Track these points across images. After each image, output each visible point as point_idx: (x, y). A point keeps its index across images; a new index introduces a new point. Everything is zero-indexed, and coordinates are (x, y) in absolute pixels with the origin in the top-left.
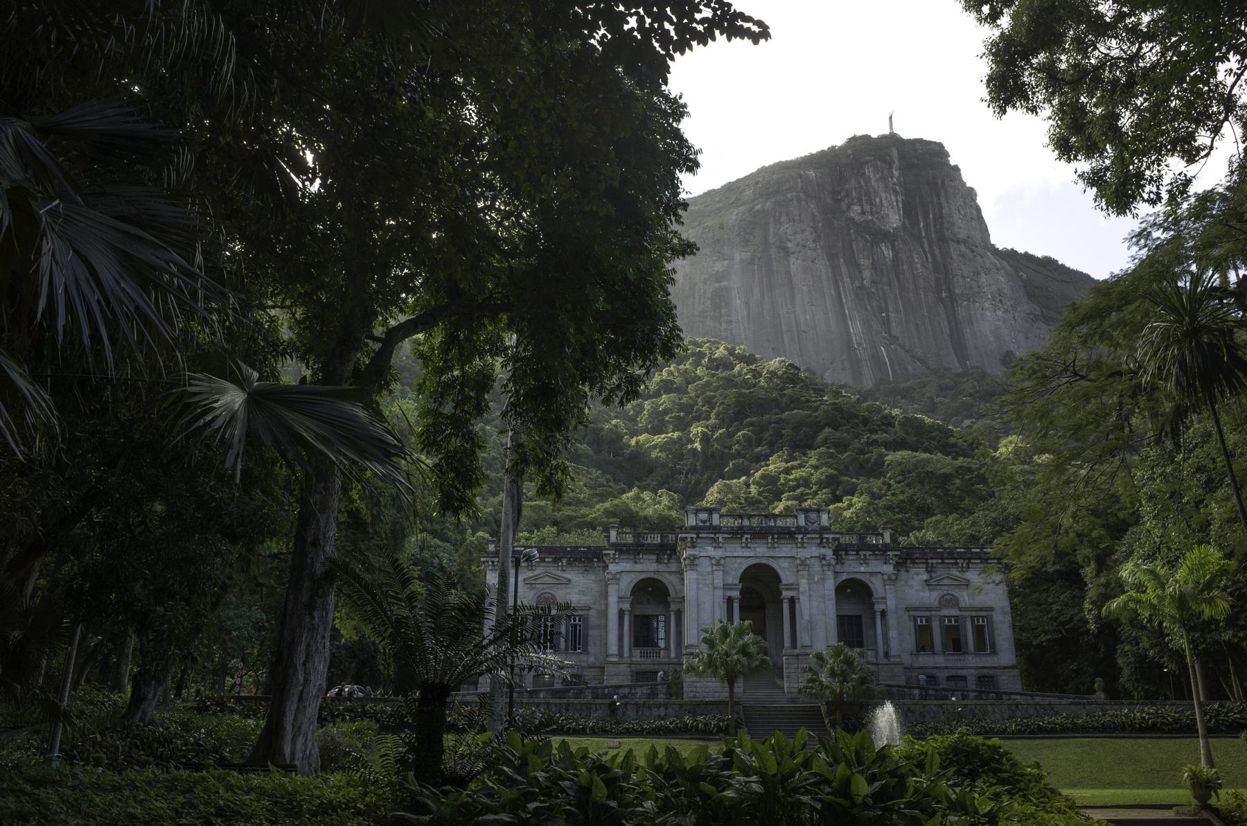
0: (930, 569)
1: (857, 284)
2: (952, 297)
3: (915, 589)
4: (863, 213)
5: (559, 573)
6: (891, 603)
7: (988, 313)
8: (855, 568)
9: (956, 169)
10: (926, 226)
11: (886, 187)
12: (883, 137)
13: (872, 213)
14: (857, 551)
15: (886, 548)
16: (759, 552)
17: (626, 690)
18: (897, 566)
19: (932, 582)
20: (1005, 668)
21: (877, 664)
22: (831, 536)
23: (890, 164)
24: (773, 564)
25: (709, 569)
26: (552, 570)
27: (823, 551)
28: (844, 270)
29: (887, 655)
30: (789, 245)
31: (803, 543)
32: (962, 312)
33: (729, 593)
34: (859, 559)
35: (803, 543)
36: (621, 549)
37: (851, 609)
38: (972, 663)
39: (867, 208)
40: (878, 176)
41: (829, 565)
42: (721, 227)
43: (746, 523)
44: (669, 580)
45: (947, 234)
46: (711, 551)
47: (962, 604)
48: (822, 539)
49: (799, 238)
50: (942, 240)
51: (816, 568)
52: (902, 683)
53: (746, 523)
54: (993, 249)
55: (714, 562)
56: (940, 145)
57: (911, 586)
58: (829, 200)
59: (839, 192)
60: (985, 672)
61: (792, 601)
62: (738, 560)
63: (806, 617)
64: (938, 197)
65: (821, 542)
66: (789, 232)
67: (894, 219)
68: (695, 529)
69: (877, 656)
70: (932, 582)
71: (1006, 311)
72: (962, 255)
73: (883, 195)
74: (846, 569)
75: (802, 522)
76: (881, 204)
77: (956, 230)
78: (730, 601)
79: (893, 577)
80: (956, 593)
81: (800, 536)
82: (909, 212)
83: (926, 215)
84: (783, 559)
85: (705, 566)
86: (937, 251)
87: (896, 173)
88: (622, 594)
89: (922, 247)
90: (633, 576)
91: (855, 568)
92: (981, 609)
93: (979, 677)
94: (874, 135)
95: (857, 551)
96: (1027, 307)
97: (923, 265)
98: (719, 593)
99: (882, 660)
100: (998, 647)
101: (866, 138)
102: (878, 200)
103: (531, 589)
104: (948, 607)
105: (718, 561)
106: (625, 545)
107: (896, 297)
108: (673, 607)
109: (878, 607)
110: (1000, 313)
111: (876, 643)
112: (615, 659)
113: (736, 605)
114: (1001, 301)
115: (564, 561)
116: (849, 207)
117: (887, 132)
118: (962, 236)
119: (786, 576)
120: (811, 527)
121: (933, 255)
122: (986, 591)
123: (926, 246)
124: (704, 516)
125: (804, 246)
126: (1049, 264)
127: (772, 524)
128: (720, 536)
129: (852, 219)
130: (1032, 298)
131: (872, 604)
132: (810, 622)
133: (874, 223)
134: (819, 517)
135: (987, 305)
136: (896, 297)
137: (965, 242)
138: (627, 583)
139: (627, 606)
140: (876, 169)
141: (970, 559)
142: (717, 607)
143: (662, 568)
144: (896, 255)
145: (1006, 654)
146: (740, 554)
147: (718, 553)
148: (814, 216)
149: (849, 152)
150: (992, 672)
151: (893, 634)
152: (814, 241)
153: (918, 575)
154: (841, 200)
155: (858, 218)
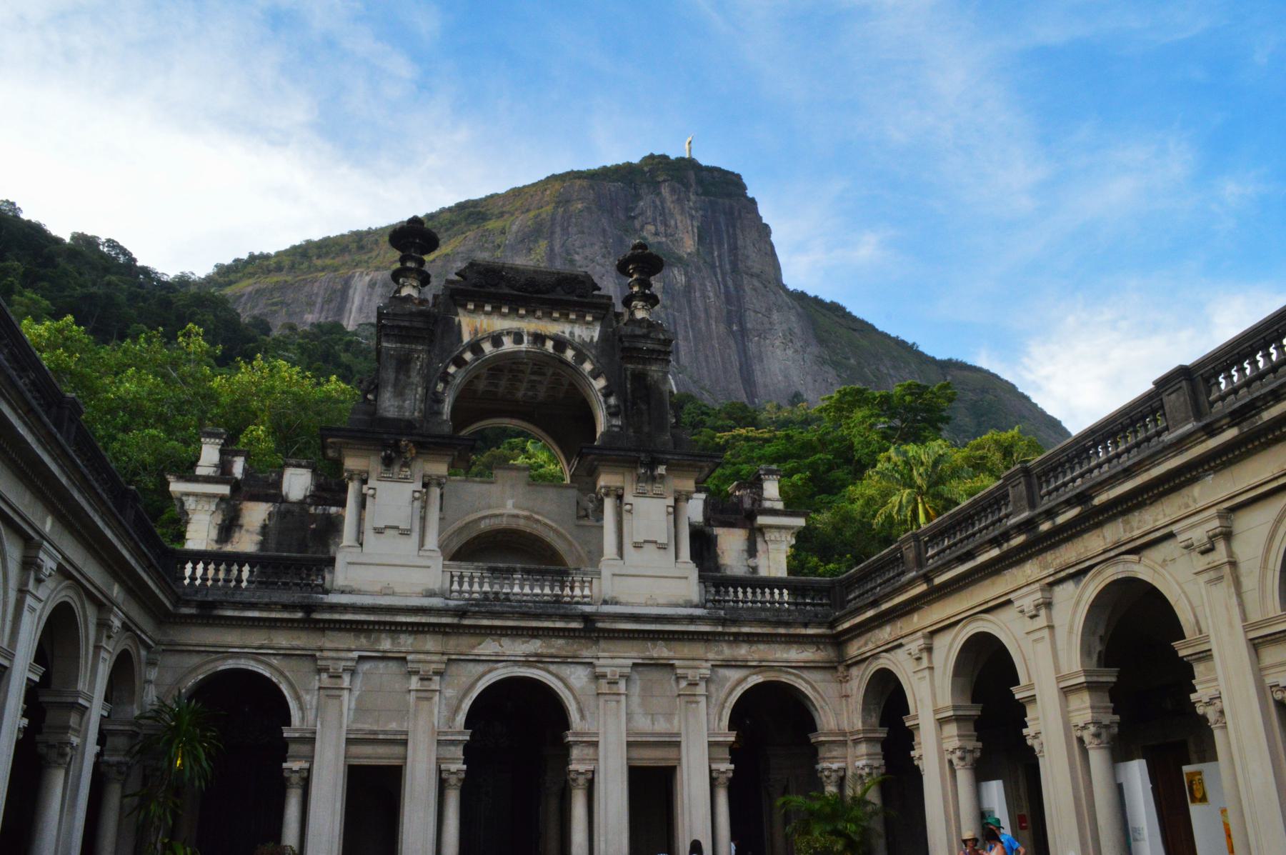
2: (743, 332)
4: (656, 234)
7: (778, 352)
9: (753, 202)
10: (719, 256)
11: (683, 210)
12: (681, 160)
13: (666, 236)
23: (687, 186)
30: (577, 257)
32: (752, 348)
39: (661, 229)
40: (675, 197)
42: (503, 232)
45: (740, 265)
49: (588, 251)
50: (735, 269)
54: (784, 288)
56: (738, 176)
58: (621, 216)
59: (633, 209)
64: (734, 227)
66: (577, 243)
67: (688, 245)
71: (796, 351)
72: (755, 289)
73: (679, 217)
76: (676, 227)
77: (750, 263)
82: (701, 240)
83: (720, 244)
86: (730, 283)
87: (693, 197)
89: (716, 275)
94: (673, 157)
96: (814, 349)
97: (717, 296)
107: (686, 326)
110: (790, 352)
114: (791, 341)
116: (642, 228)
118: (754, 270)
121: (726, 286)
123: (719, 276)
125: (592, 261)
126: (835, 309)
130: (821, 341)
135: (777, 343)
136: (686, 326)
137: (758, 276)
140: (673, 191)
144: (689, 279)
148: (604, 231)
149: (646, 169)
154: (634, 218)
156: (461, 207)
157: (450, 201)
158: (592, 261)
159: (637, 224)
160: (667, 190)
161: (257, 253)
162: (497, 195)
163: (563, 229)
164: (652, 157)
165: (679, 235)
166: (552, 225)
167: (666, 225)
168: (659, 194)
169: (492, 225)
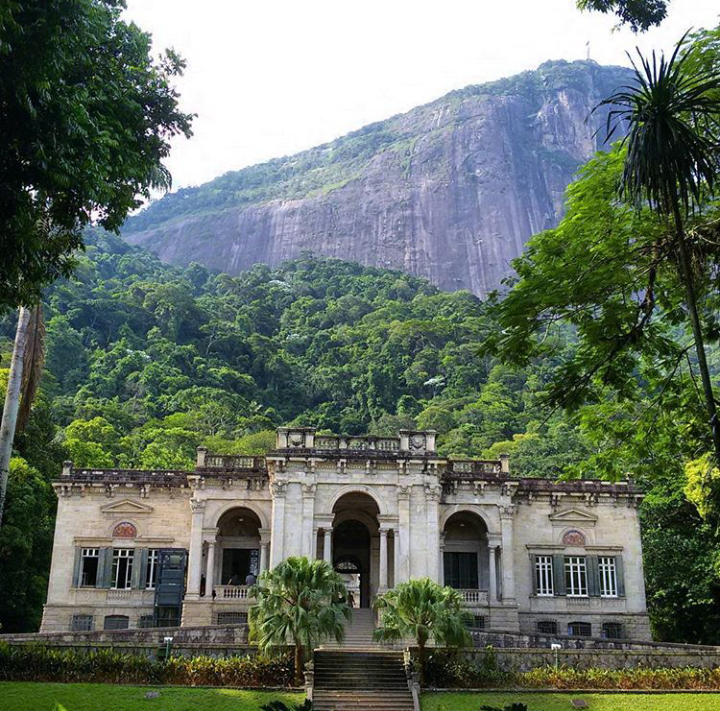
0: (554, 503)
1: (547, 216)
3: (539, 524)
4: (555, 143)
5: (142, 501)
6: (506, 541)
8: (466, 500)
14: (471, 481)
15: (504, 477)
16: (356, 479)
17: (198, 634)
18: (513, 500)
19: (556, 517)
20: (633, 615)
21: (488, 607)
22: (436, 462)
24: (372, 492)
25: (299, 497)
26: (134, 498)
27: (427, 478)
28: (534, 202)
29: (500, 598)
31: (405, 470)
33: (321, 524)
34: (472, 489)
35: (405, 470)
36: (205, 473)
37: (462, 546)
38: (598, 610)
41: (434, 494)
43: (343, 446)
44: (257, 508)
46: (301, 476)
47: (589, 543)
48: (426, 465)
51: (419, 496)
52: (517, 630)
53: (343, 446)
55: (305, 489)
57: (533, 521)
60: (611, 619)
61: (391, 535)
62: (332, 488)
63: (405, 553)
65: (426, 469)
68: (287, 453)
69: (488, 598)
70: (556, 517)
74: (459, 501)
75: (405, 445)
78: (321, 534)
79: (510, 510)
80: (582, 529)
81: (402, 462)
84: (383, 488)
85: (295, 493)
88: (207, 525)
90: (220, 504)
91: (466, 500)
92: (610, 549)
93: (604, 624)
95: (471, 481)
98: (309, 524)
99: (494, 602)
100: (628, 591)
101: (563, 63)
102: (571, 130)
103: (108, 519)
104: (572, 545)
105: (310, 487)
106: (214, 470)
108: (264, 540)
109: (493, 544)
111: (489, 585)
112: (196, 598)
113: (328, 539)
115: (148, 487)
117: (583, 57)
119: (385, 506)
120: (415, 452)
122: (618, 530)
124: (296, 437)
127: (373, 447)
128: (313, 460)
129: (543, 148)
131: (487, 543)
132: (410, 557)
133: (567, 153)
134: (425, 441)
138: (215, 512)
139: (212, 539)
140: (570, 98)
141: (598, 493)
142: (305, 537)
143: (254, 496)
145: (636, 600)
146: (335, 481)
147: (309, 480)
148: (503, 144)
150: (619, 619)
151: (508, 574)
152: (504, 170)
153: (541, 509)
155: (550, 148)
156: (367, 130)
157: (357, 126)
158: (493, 176)
159: (535, 134)
160: (565, 97)
161: (185, 187)
162: (401, 115)
163: (464, 147)
164: (549, 64)
165: (578, 140)
166: (453, 144)
167: (564, 133)
168: (558, 101)
169: (396, 147)
